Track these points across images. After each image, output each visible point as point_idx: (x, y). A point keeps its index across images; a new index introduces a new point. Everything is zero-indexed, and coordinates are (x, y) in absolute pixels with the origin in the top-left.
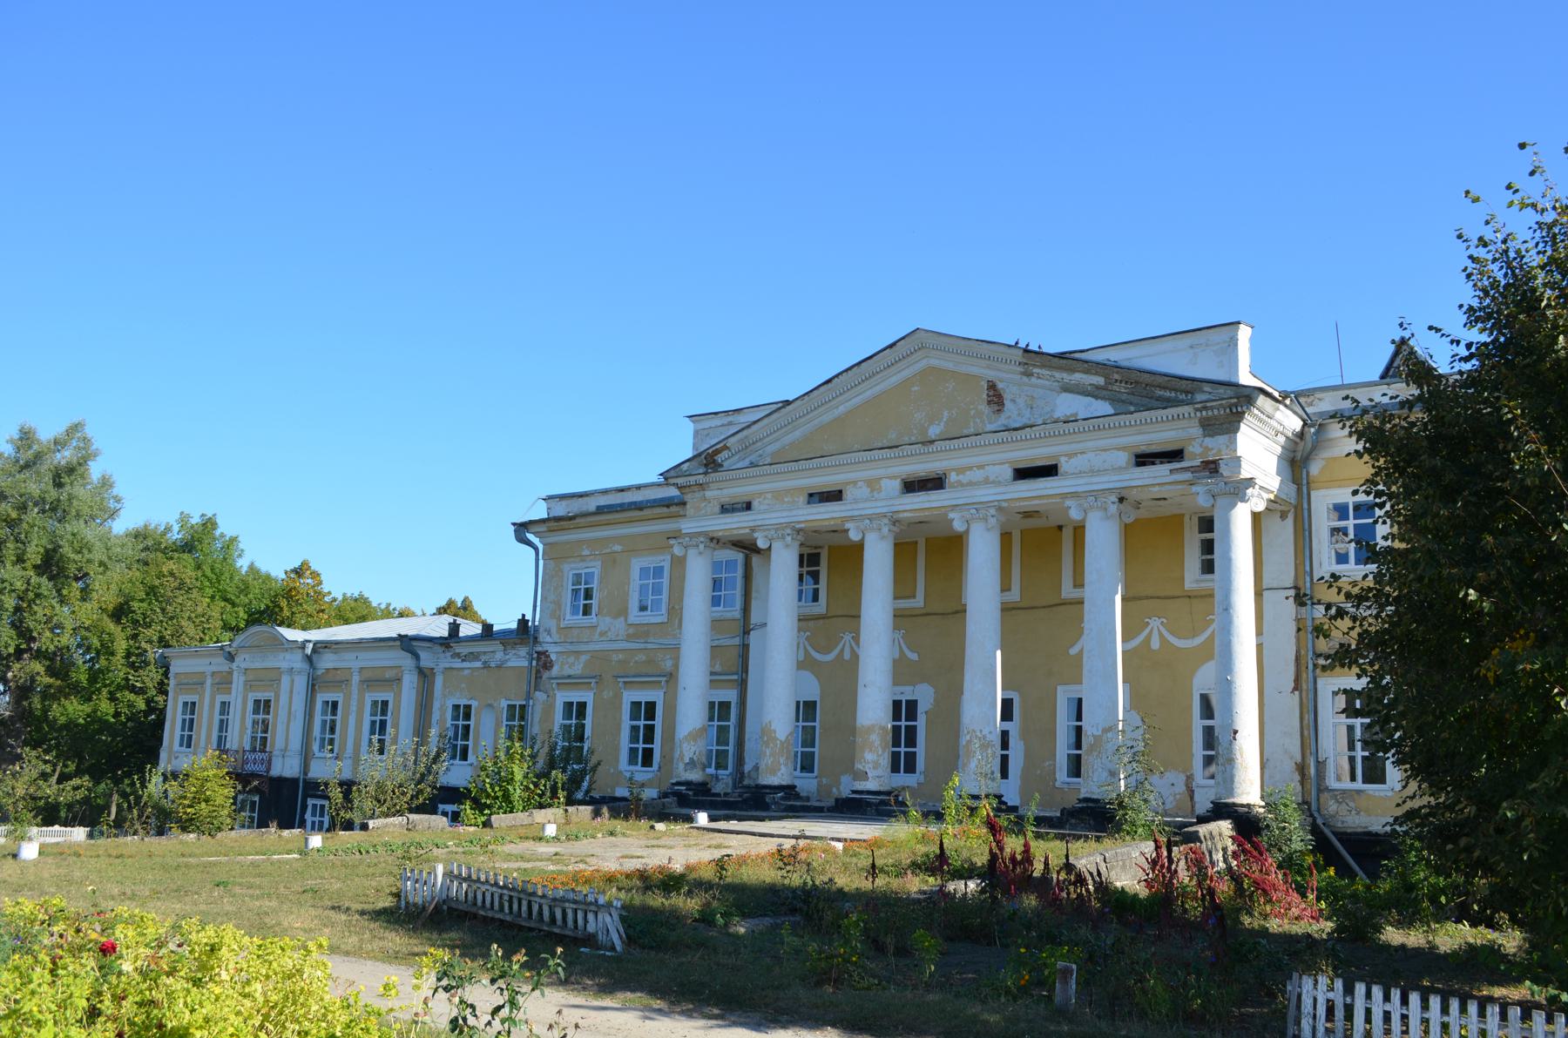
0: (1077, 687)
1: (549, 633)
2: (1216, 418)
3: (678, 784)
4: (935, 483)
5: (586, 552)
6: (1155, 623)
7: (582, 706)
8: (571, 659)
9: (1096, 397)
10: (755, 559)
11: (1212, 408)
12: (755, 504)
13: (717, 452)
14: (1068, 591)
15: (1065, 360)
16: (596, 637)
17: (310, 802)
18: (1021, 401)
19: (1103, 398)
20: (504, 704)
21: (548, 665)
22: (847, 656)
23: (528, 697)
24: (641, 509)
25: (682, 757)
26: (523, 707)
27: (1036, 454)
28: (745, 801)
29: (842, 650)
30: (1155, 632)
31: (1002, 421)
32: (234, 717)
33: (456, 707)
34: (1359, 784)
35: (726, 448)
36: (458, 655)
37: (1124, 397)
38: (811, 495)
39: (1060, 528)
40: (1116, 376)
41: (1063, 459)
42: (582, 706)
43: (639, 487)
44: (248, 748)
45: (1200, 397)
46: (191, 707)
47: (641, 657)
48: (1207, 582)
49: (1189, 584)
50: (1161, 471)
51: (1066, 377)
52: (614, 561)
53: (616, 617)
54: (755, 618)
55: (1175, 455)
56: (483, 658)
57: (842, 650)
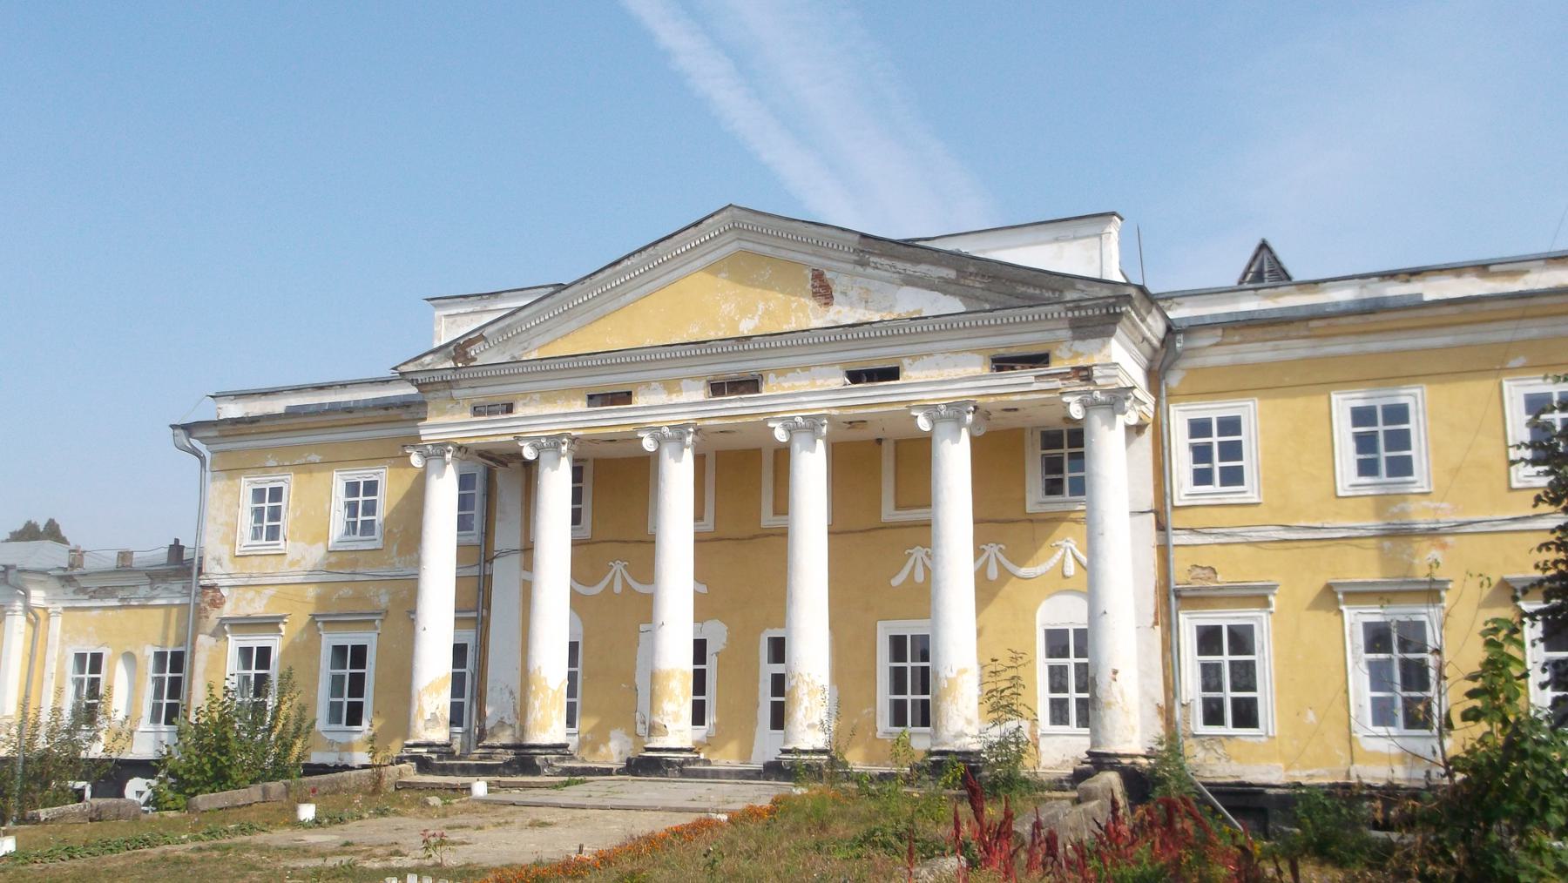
0: (926, 622)
1: (219, 561)
2: (1087, 316)
4: (750, 385)
5: (272, 463)
8: (250, 593)
9: (945, 293)
10: (500, 473)
11: (1086, 308)
13: (471, 342)
15: (909, 249)
19: (953, 294)
20: (150, 652)
21: (217, 603)
22: (919, 577)
25: (421, 712)
26: (1081, 635)
27: (875, 357)
28: (508, 764)
29: (612, 582)
33: (80, 658)
34: (1228, 729)
35: (482, 337)
36: (84, 590)
37: (978, 293)
38: (591, 397)
39: (879, 441)
40: (972, 269)
41: (906, 362)
43: (344, 385)
45: (1070, 295)
47: (346, 591)
48: (1056, 504)
49: (1030, 508)
50: (1024, 378)
51: (910, 268)
55: (1040, 359)
56: (121, 594)
57: (612, 582)
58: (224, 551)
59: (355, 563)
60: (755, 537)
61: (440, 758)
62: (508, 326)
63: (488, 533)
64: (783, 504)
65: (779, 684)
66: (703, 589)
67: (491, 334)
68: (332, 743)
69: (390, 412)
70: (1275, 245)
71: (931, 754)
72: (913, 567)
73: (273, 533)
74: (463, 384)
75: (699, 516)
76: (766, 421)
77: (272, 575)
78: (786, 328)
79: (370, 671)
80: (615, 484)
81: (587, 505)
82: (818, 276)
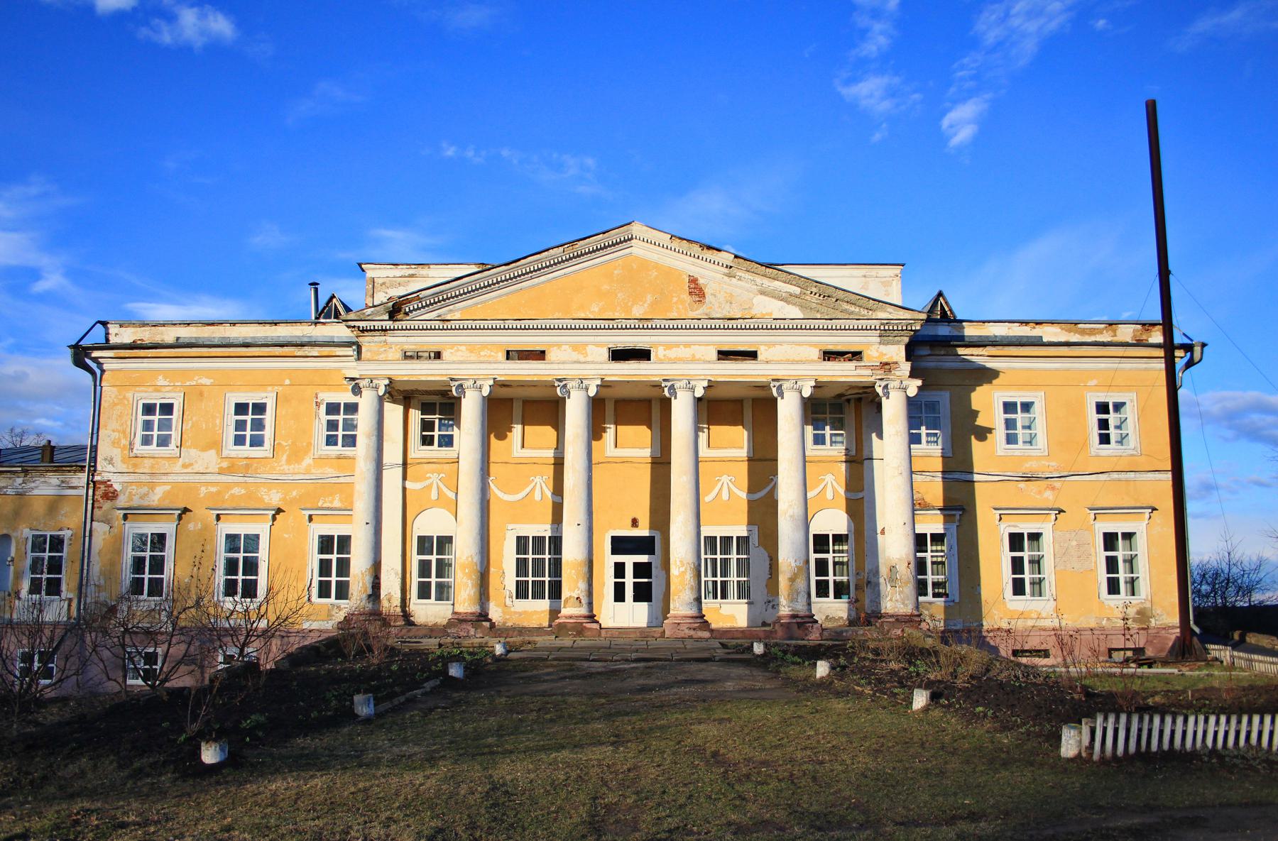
1: (111, 461)
6: (725, 479)
9: (788, 303)
12: (445, 355)
16: (178, 468)
24: (282, 346)
40: (814, 290)
51: (766, 282)
52: (201, 394)
53: (205, 449)
55: (856, 355)
58: (116, 453)
70: (945, 294)
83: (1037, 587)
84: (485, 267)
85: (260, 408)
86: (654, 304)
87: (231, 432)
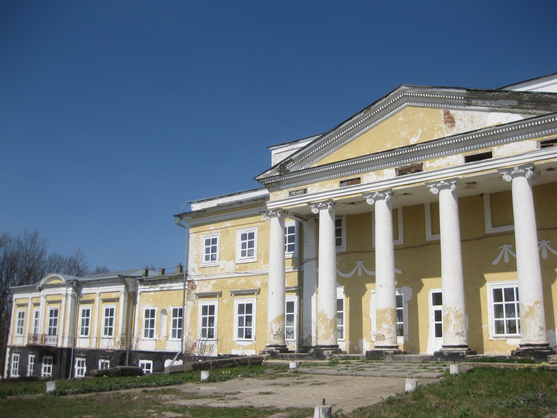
1: (194, 271)
3: (271, 346)
4: (418, 169)
7: (212, 308)
8: (206, 283)
14: (489, 229)
16: (219, 271)
17: (77, 359)
18: (465, 119)
21: (193, 288)
23: (184, 305)
28: (311, 355)
29: (357, 271)
30: (544, 249)
31: (454, 131)
32: (41, 318)
33: (147, 311)
38: (341, 182)
39: (482, 195)
42: (212, 308)
44: (47, 333)
46: (22, 315)
52: (227, 232)
53: (230, 260)
54: (306, 256)
57: (357, 271)
59: (246, 268)
60: (423, 245)
61: (281, 352)
62: (303, 154)
63: (301, 252)
64: (436, 230)
65: (438, 315)
66: (399, 272)
67: (296, 158)
68: (240, 346)
69: (258, 202)
71: (521, 346)
72: (503, 255)
73: (213, 259)
74: (284, 182)
75: (395, 236)
76: (427, 184)
77: (214, 275)
78: (432, 139)
79: (254, 315)
80: (354, 224)
81: (344, 237)
82: (447, 114)
83: (512, 326)
84: (324, 135)
85: (252, 235)
86: (423, 133)
87: (239, 250)
